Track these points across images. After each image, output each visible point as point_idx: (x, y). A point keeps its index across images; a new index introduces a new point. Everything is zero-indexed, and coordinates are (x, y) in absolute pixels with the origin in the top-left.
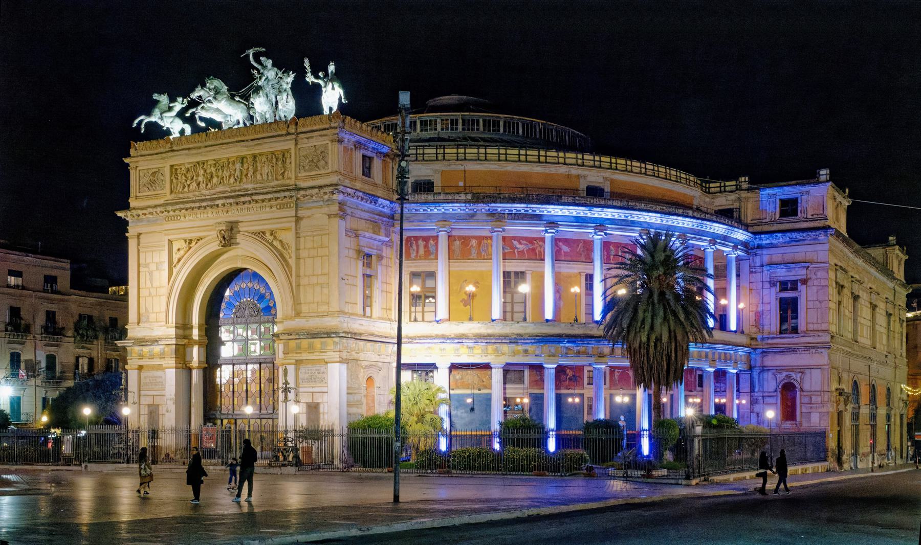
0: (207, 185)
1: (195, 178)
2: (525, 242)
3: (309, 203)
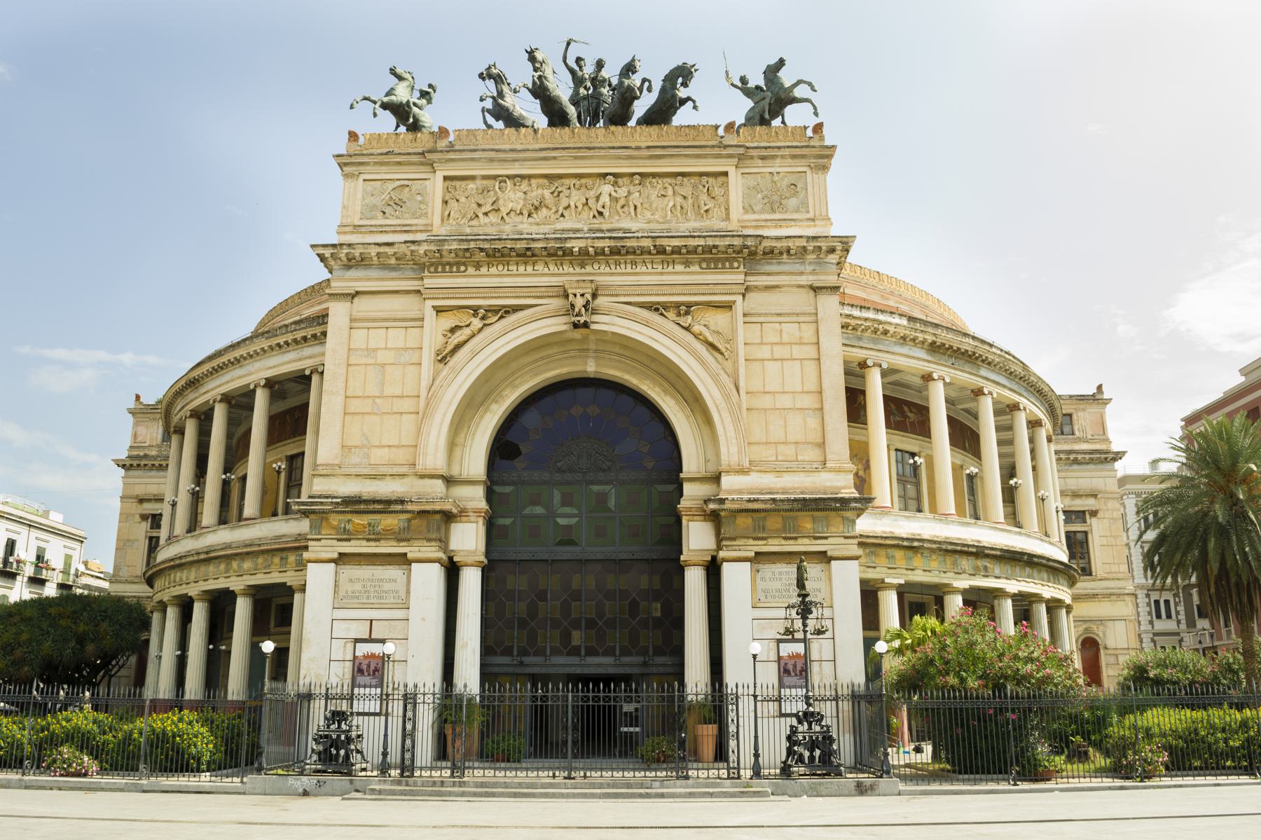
0: (529, 216)
1: (501, 202)
2: (914, 410)
3: (771, 263)
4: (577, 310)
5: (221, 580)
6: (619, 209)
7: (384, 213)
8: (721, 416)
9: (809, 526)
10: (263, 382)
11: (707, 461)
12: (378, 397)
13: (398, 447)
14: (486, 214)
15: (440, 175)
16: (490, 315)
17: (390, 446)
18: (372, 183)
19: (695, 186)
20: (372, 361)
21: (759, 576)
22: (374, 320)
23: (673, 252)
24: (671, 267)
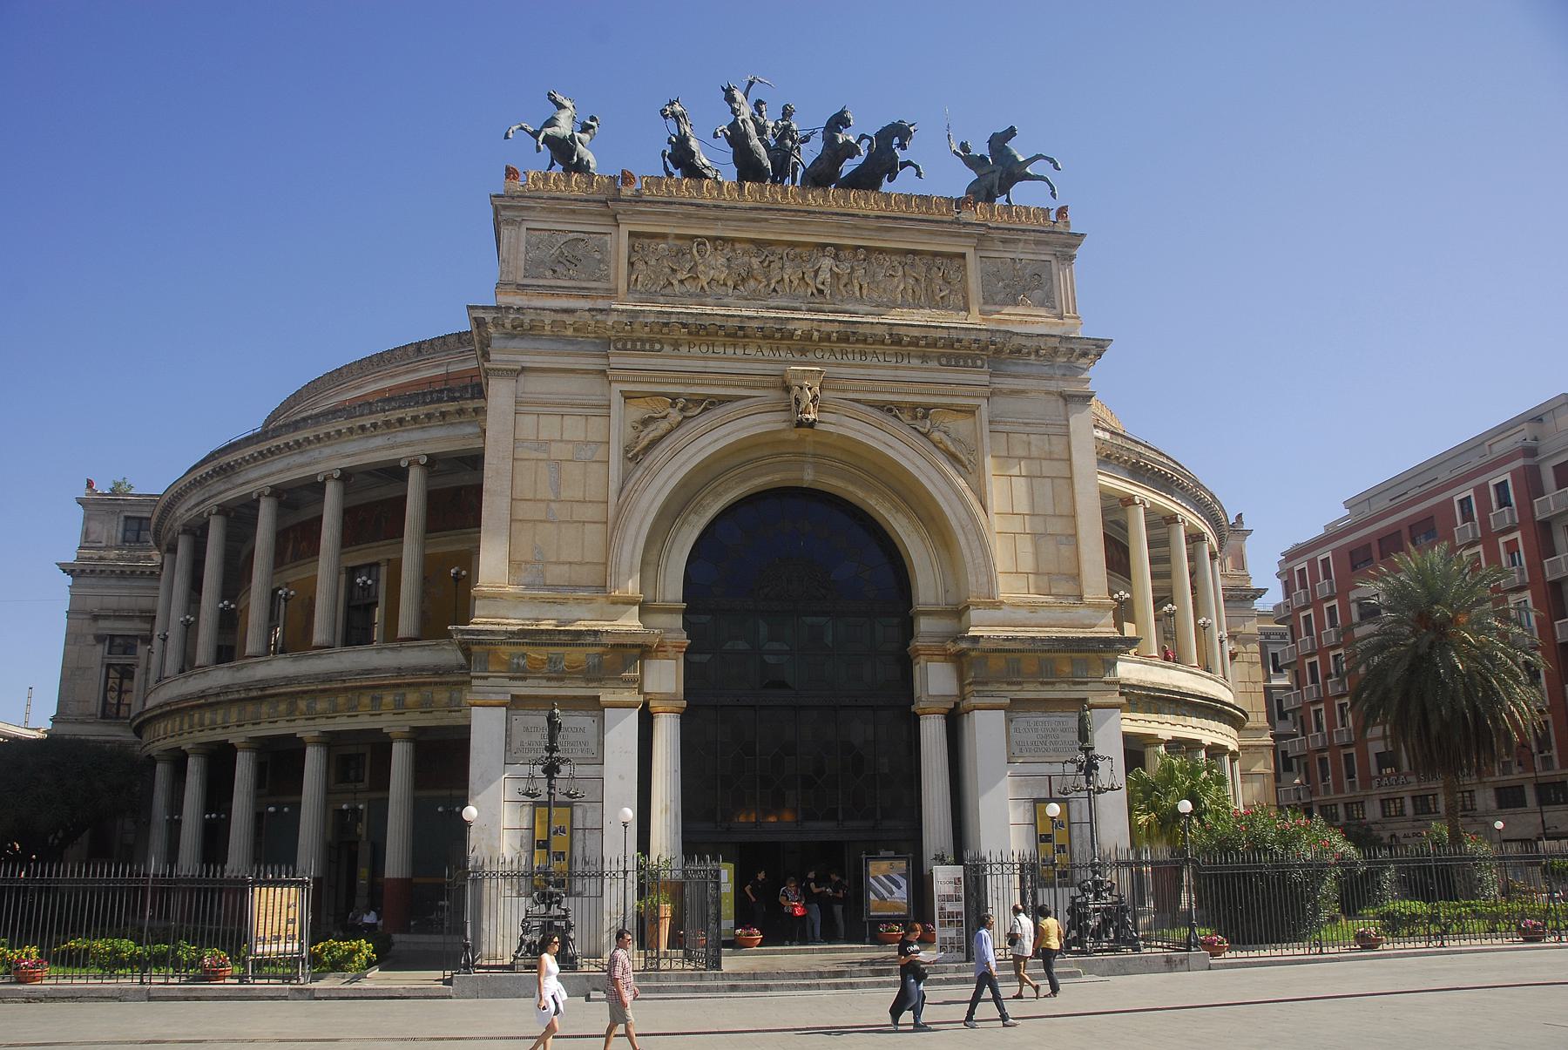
1: (701, 268)
3: (1017, 364)
4: (803, 406)
5: (282, 724)
6: (841, 287)
7: (554, 271)
8: (967, 539)
9: (1067, 669)
10: (337, 474)
11: (947, 591)
12: (554, 501)
13: (580, 564)
14: (681, 282)
15: (624, 230)
16: (691, 406)
17: (570, 563)
18: (537, 233)
19: (929, 270)
20: (545, 456)
21: (1012, 726)
22: (545, 404)
23: (910, 344)
24: (906, 361)
